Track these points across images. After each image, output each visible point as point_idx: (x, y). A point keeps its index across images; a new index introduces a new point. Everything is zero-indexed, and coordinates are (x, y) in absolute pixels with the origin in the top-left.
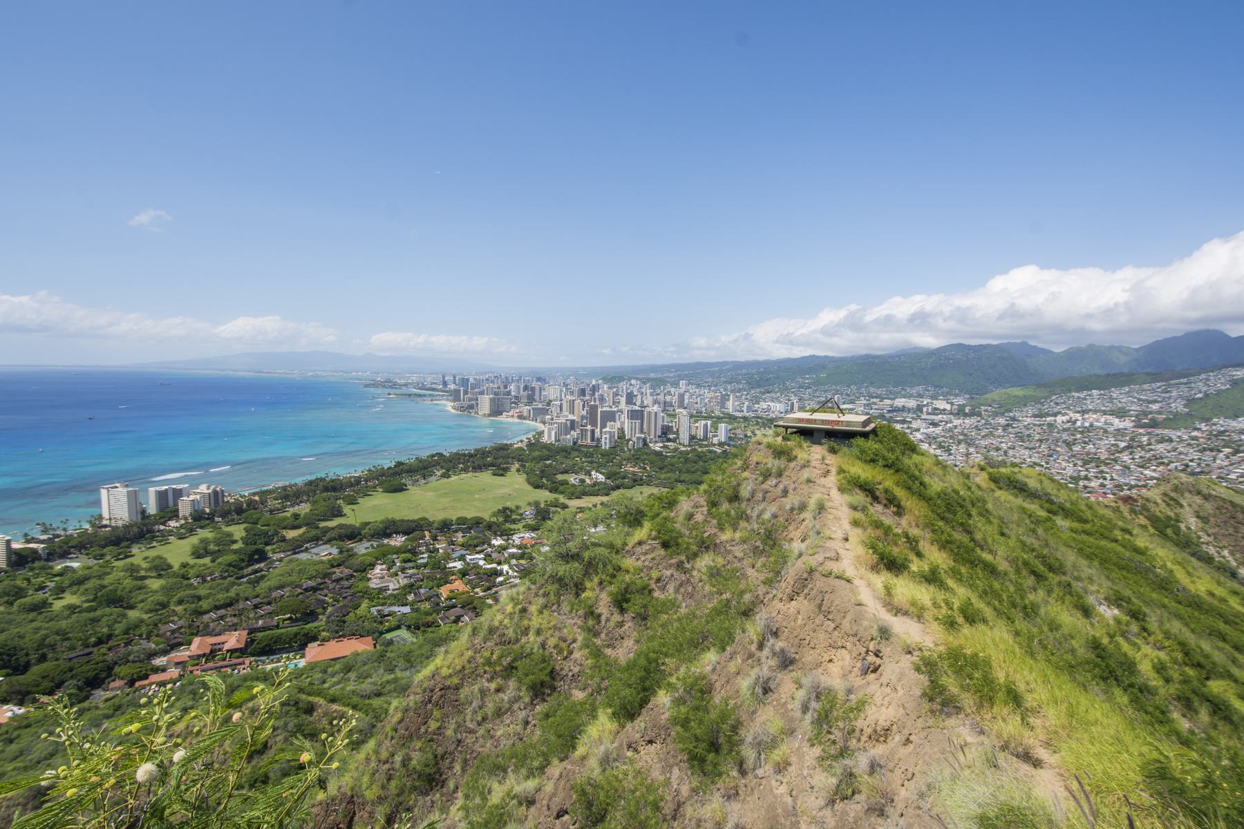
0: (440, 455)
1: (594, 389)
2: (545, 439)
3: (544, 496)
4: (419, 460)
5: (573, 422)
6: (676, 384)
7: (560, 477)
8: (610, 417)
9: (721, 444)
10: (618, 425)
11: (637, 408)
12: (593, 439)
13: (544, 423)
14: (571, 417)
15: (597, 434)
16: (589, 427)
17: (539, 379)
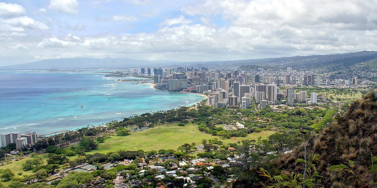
1: (236, 73)
2: (208, 104)
3: (209, 137)
4: (137, 117)
5: (224, 93)
6: (285, 69)
7: (217, 126)
8: (246, 90)
9: (313, 105)
10: (251, 94)
11: (262, 84)
12: (236, 104)
13: (207, 94)
14: (223, 91)
16: (234, 96)
17: (203, 68)
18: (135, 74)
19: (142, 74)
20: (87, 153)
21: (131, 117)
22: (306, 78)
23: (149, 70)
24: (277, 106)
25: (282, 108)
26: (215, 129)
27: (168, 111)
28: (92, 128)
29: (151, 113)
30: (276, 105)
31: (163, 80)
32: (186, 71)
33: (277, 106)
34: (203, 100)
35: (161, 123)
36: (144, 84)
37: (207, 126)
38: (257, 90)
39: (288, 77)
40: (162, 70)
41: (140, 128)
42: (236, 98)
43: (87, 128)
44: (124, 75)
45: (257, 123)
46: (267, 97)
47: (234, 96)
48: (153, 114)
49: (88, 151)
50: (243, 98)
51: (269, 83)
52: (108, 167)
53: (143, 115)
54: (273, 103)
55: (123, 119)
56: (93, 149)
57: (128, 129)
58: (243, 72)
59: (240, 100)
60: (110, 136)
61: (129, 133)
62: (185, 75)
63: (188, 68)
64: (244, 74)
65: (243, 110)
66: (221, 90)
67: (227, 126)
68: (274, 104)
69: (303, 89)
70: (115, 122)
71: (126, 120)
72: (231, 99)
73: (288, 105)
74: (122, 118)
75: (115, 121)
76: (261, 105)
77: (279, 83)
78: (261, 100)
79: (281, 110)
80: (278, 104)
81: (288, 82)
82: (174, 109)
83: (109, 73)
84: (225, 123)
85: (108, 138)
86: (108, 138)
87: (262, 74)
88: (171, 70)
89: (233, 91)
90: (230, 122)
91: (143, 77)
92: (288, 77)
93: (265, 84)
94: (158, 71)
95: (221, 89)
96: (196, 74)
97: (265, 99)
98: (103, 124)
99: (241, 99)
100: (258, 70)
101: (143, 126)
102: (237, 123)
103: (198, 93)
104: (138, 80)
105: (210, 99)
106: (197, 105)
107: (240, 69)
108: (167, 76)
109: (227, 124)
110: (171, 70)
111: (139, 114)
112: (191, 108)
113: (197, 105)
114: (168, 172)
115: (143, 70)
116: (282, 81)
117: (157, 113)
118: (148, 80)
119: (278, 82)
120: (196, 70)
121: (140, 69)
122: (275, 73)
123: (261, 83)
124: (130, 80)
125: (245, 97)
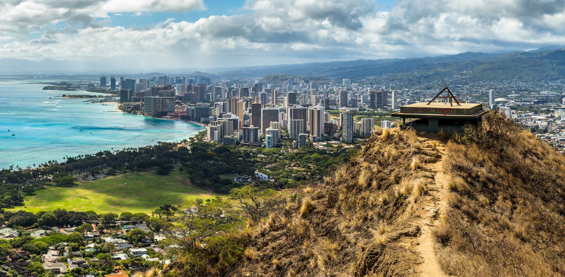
0: (108, 153)
1: (257, 88)
2: (207, 139)
4: (89, 157)
5: (235, 121)
7: (223, 177)
8: (273, 115)
14: (233, 117)
15: (260, 134)
16: (251, 127)
18: (91, 88)
19: (101, 86)
20: (6, 210)
21: (79, 156)
22: (374, 96)
23: (113, 81)
24: (325, 143)
25: (333, 147)
26: (219, 182)
27: (140, 149)
28: (17, 170)
29: (112, 152)
30: (323, 141)
31: (135, 96)
32: (173, 83)
33: (325, 143)
34: (199, 132)
35: (127, 168)
36: (104, 103)
37: (205, 177)
38: (291, 117)
39: (344, 95)
40: (134, 81)
41: (93, 175)
42: (256, 131)
43: (9, 171)
44: (73, 87)
45: (291, 172)
46: (309, 128)
47: (251, 127)
48: (115, 153)
49: (6, 207)
50: (267, 130)
51: (311, 105)
52: (37, 234)
53: (100, 154)
54: (317, 138)
55: (66, 160)
56: (17, 205)
57: (75, 176)
58: (269, 86)
59: (262, 133)
60: (45, 186)
61: (75, 182)
62: (171, 89)
63: (177, 78)
64: (271, 90)
65: (266, 150)
66: (230, 116)
67: (239, 176)
68: (319, 141)
69: (369, 115)
70: (54, 163)
71: (71, 160)
72: (247, 132)
73: (344, 142)
74: (66, 158)
75: (53, 161)
76: (298, 142)
77: (329, 105)
78: (298, 133)
79: (332, 151)
80: (327, 140)
81: (344, 104)
82: (151, 146)
83: (50, 83)
84: (235, 172)
85: (41, 188)
86: (41, 188)
87: (300, 88)
88: (148, 81)
89: (251, 119)
90: (244, 171)
91: (103, 91)
92: (344, 95)
93: (305, 106)
94: (128, 83)
95: (230, 114)
96: (189, 87)
97: (305, 131)
98: (34, 165)
99: (264, 132)
100: (294, 84)
101: (98, 173)
102: (256, 173)
103: (193, 120)
104: (95, 96)
105: (212, 130)
106: (189, 140)
107: (265, 81)
108: (142, 91)
109: (240, 173)
110: (148, 81)
111: (93, 152)
112: (179, 146)
113: (189, 140)
114: (133, 250)
115: (103, 80)
116: (335, 101)
117: (122, 152)
118: (110, 97)
119: (328, 103)
120: (191, 81)
121: (99, 78)
122: (323, 88)
123: (299, 104)
124: (81, 97)
125: (271, 129)
